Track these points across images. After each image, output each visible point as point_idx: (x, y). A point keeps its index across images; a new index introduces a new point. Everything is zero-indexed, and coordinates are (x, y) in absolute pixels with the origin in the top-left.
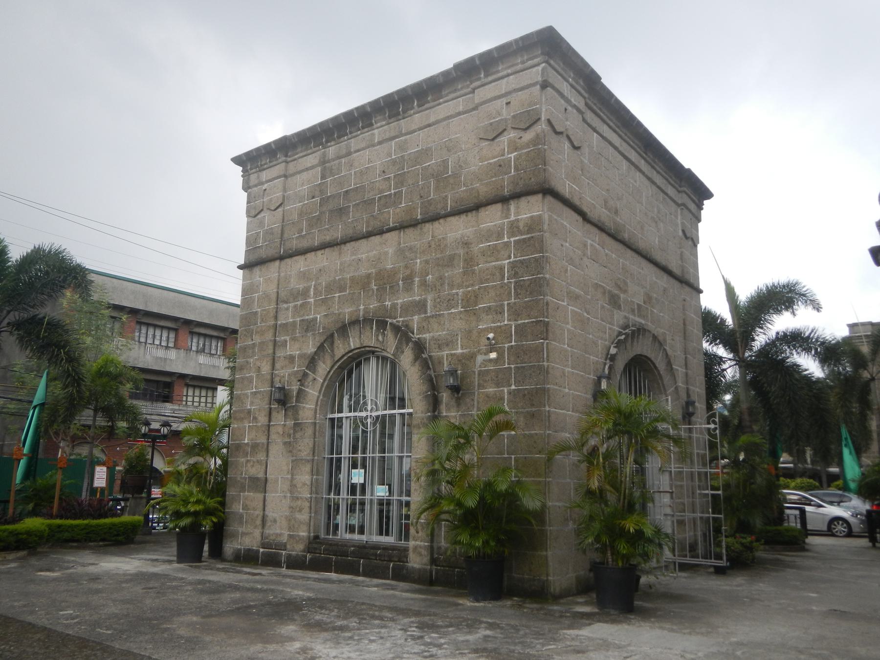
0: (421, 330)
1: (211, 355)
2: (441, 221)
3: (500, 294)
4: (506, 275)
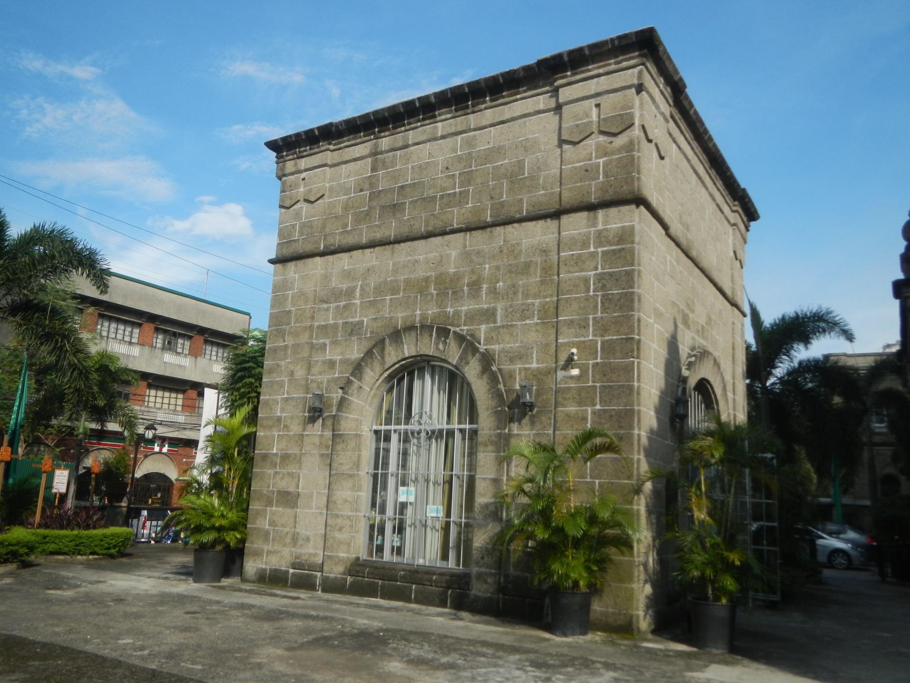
1: (178, 354)
2: (516, 225)
3: (584, 308)
4: (592, 287)
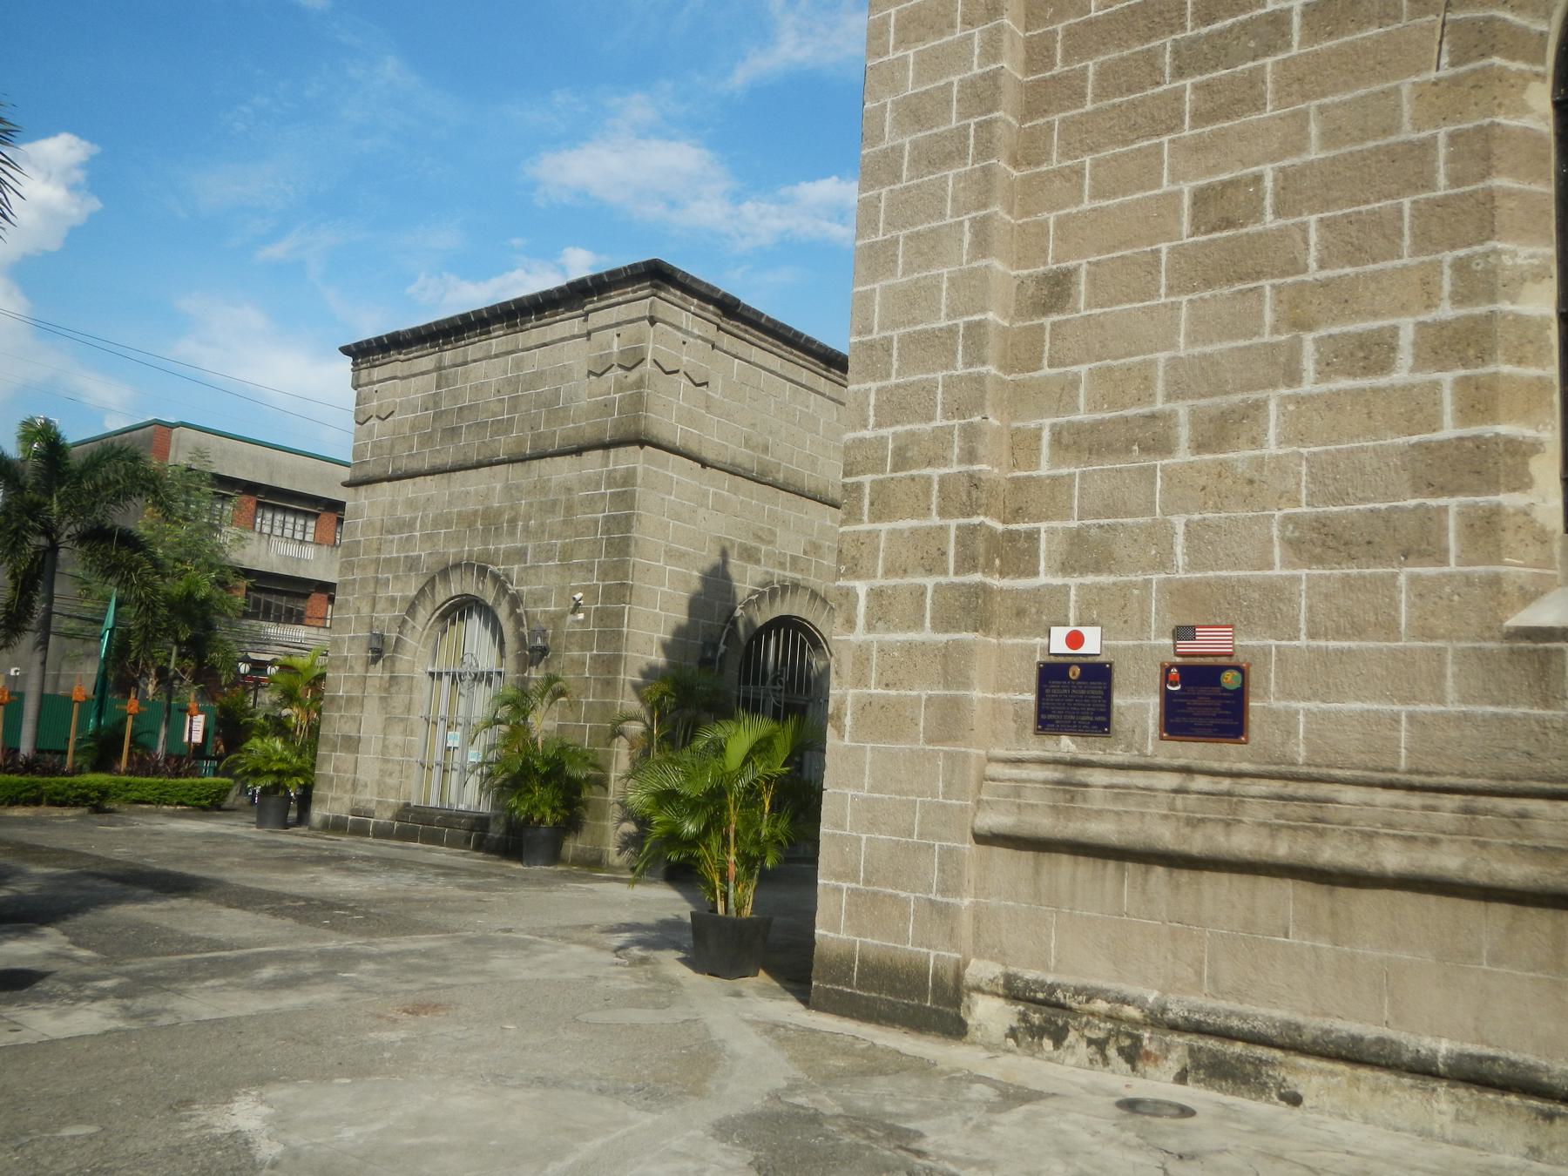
0: (521, 582)
